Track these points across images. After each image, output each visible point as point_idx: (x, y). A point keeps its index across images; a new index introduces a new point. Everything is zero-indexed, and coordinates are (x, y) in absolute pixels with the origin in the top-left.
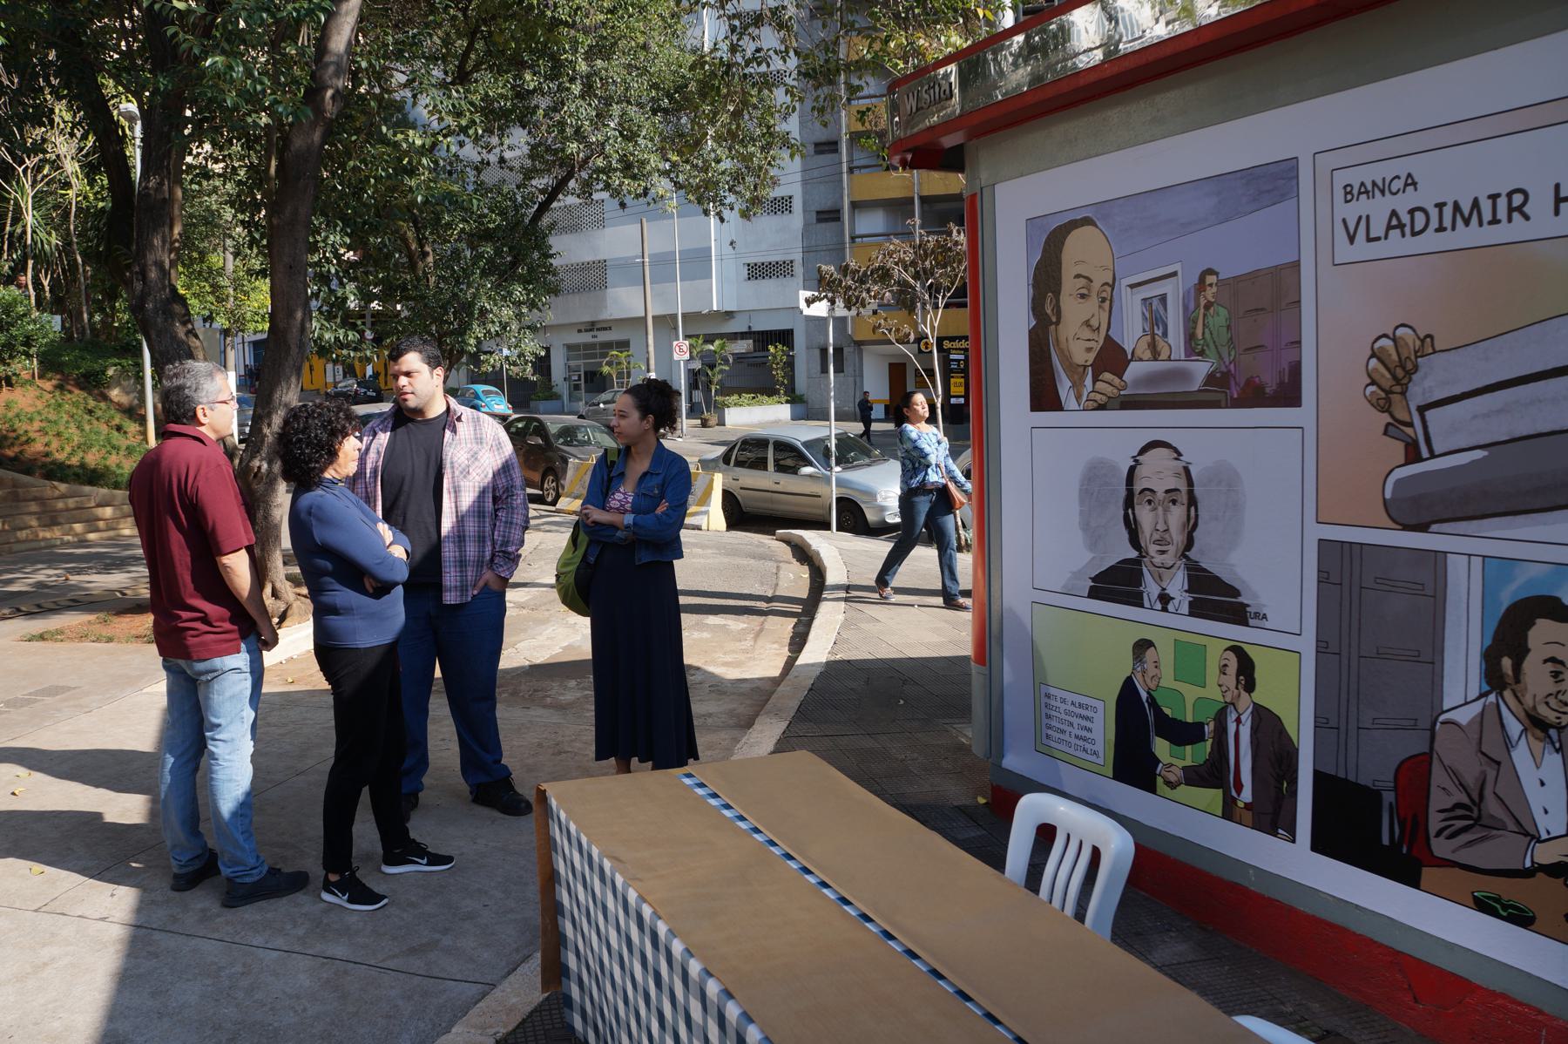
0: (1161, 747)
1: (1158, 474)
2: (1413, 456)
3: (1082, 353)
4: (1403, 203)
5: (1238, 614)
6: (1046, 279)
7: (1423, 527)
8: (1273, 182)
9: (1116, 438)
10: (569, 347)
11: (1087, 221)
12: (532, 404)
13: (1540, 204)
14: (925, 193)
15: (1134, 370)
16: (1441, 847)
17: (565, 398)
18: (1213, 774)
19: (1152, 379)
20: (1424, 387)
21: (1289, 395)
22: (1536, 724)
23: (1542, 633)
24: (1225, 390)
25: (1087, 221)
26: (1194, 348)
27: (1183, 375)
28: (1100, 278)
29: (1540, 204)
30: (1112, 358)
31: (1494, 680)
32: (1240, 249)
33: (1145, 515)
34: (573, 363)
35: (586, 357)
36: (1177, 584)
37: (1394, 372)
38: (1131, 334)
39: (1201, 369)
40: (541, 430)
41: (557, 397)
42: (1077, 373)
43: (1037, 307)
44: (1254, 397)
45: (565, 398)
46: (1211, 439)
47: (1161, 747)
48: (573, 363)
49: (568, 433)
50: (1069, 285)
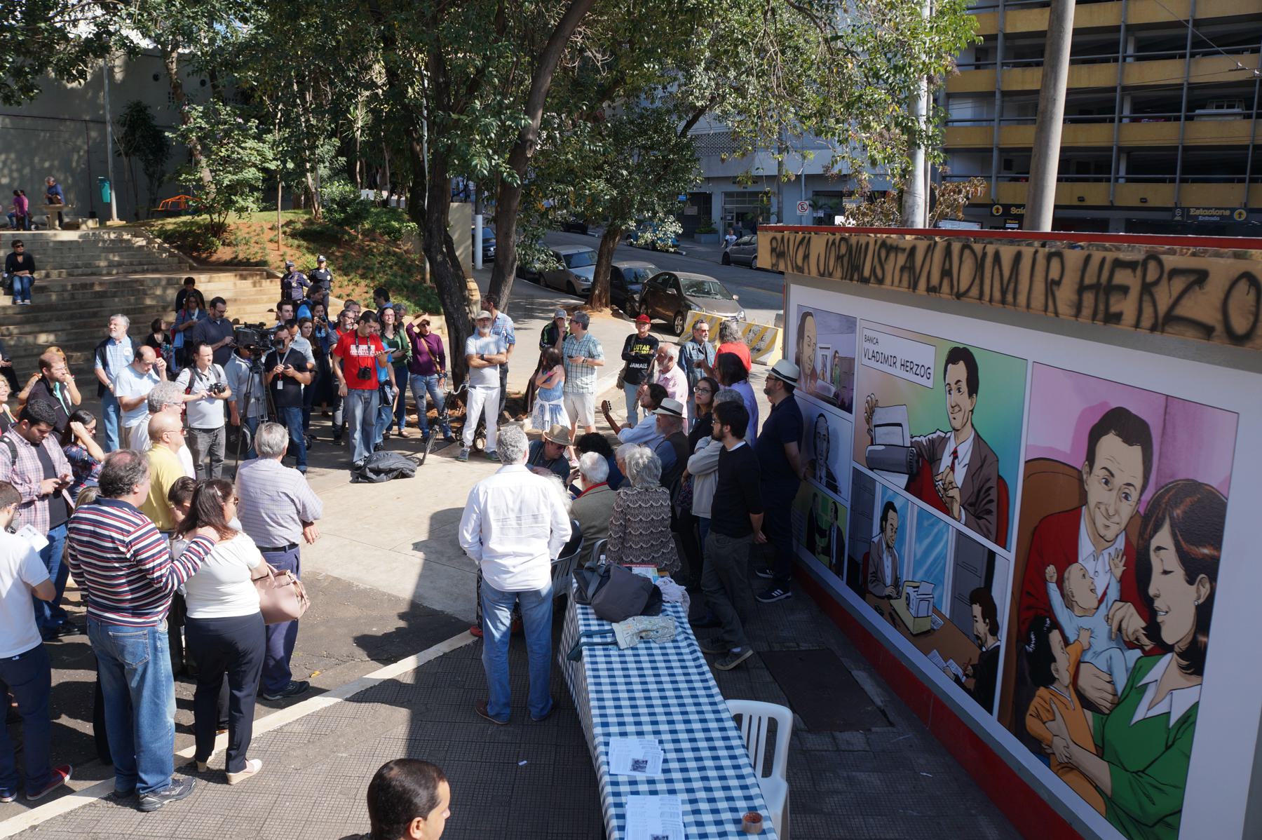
0: (817, 537)
2: (872, 444)
3: (808, 372)
4: (876, 348)
5: (835, 489)
7: (872, 469)
8: (849, 324)
10: (728, 195)
11: (810, 314)
12: (696, 236)
13: (898, 364)
14: (1006, 89)
15: (819, 381)
16: (870, 586)
17: (721, 232)
18: (827, 551)
19: (824, 388)
20: (877, 419)
21: (849, 409)
22: (888, 546)
23: (891, 513)
25: (810, 314)
26: (832, 382)
27: (829, 390)
28: (814, 341)
29: (898, 364)
31: (883, 530)
34: (728, 206)
35: (737, 202)
36: (824, 474)
37: (871, 411)
39: (833, 389)
40: (676, 283)
41: (715, 232)
45: (721, 232)
47: (817, 537)
48: (728, 206)
49: (699, 288)
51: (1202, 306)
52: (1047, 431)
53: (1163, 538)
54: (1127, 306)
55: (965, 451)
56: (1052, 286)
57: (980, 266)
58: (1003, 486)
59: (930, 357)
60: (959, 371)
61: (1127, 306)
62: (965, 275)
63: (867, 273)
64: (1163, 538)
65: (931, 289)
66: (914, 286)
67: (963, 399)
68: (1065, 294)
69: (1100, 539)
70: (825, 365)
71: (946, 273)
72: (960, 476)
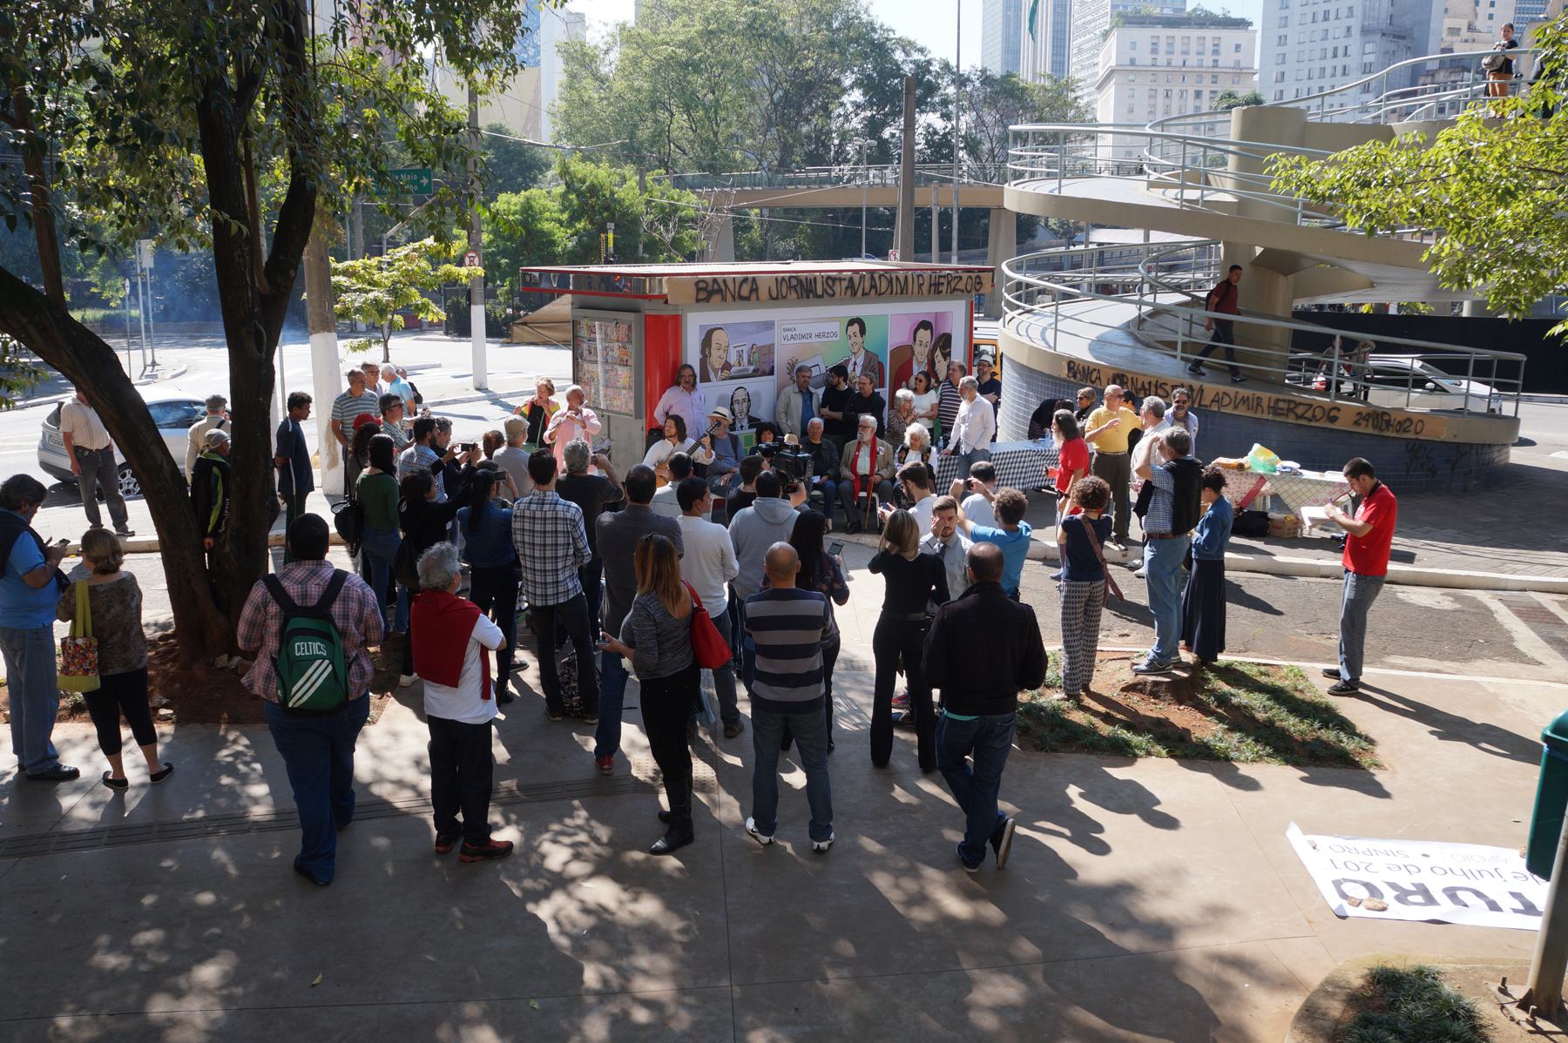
1: (740, 395)
3: (718, 365)
6: (706, 343)
8: (769, 325)
9: (729, 387)
21: (771, 373)
24: (757, 373)
26: (750, 363)
30: (727, 366)
32: (761, 340)
33: (736, 407)
36: (745, 423)
38: (733, 359)
42: (716, 371)
43: (703, 352)
44: (764, 374)
46: (752, 385)
50: (714, 345)
51: (961, 286)
52: (898, 337)
53: (938, 352)
54: (943, 288)
55: (860, 360)
56: (920, 286)
57: (890, 282)
58: (881, 365)
59: (836, 327)
60: (856, 327)
61: (943, 288)
62: (884, 284)
63: (819, 292)
64: (938, 352)
65: (864, 294)
66: (854, 294)
67: (859, 339)
68: (925, 288)
69: (920, 363)
70: (740, 356)
71: (873, 286)
72: (859, 370)
